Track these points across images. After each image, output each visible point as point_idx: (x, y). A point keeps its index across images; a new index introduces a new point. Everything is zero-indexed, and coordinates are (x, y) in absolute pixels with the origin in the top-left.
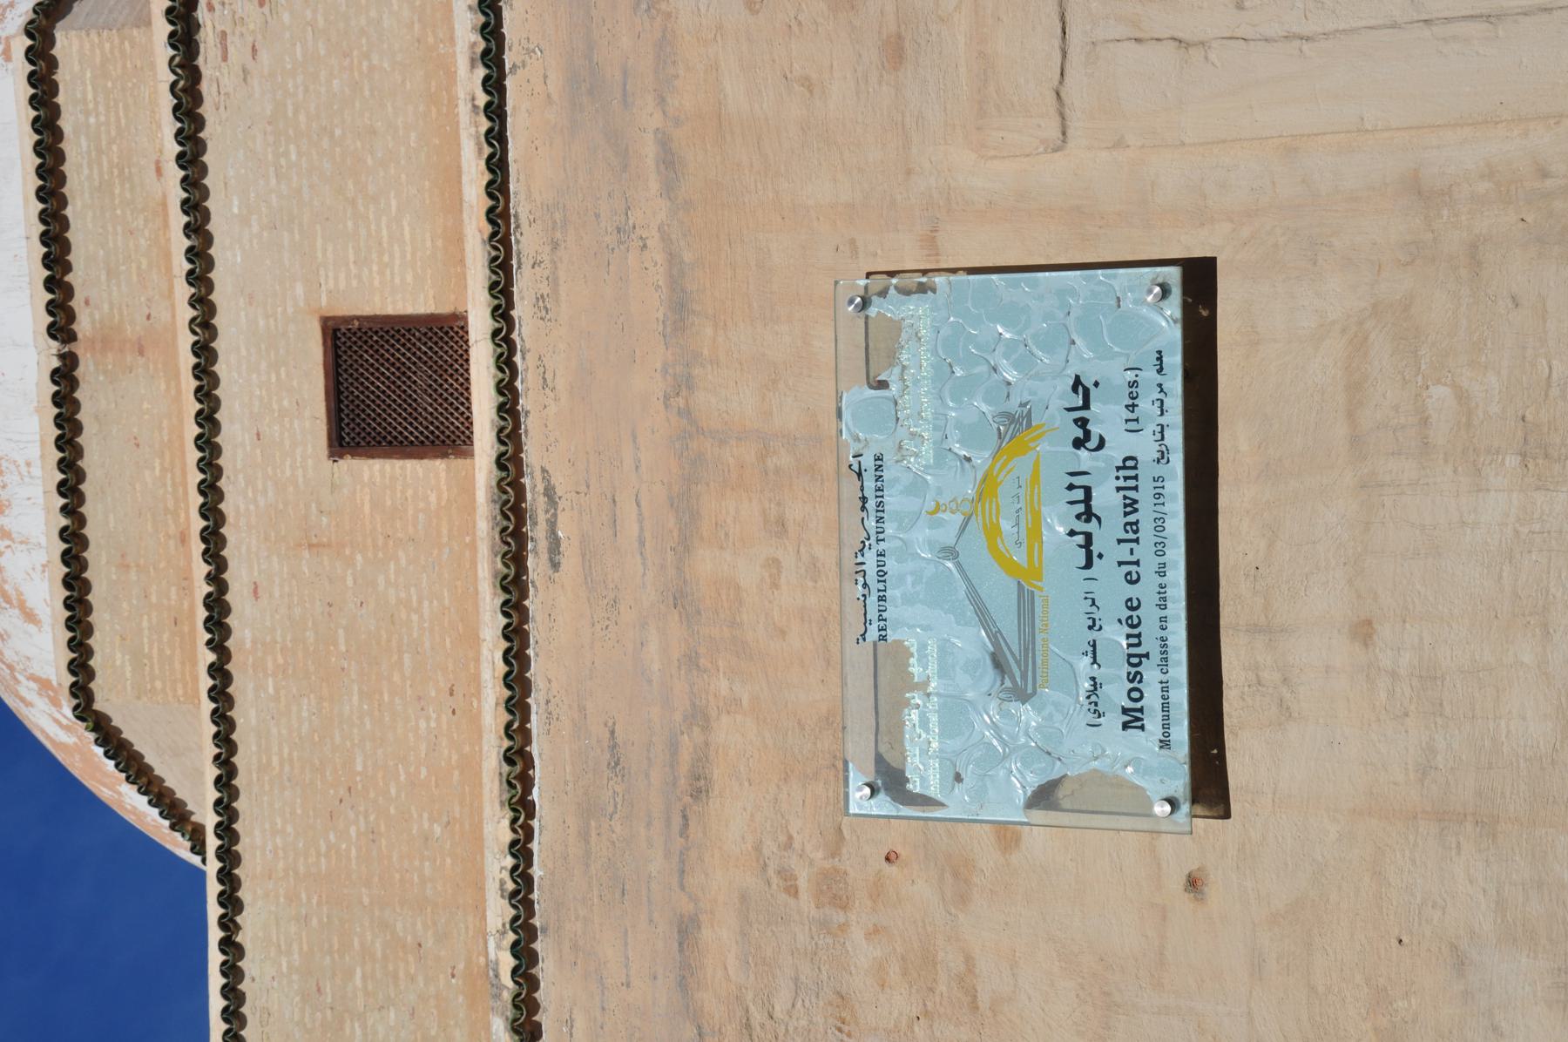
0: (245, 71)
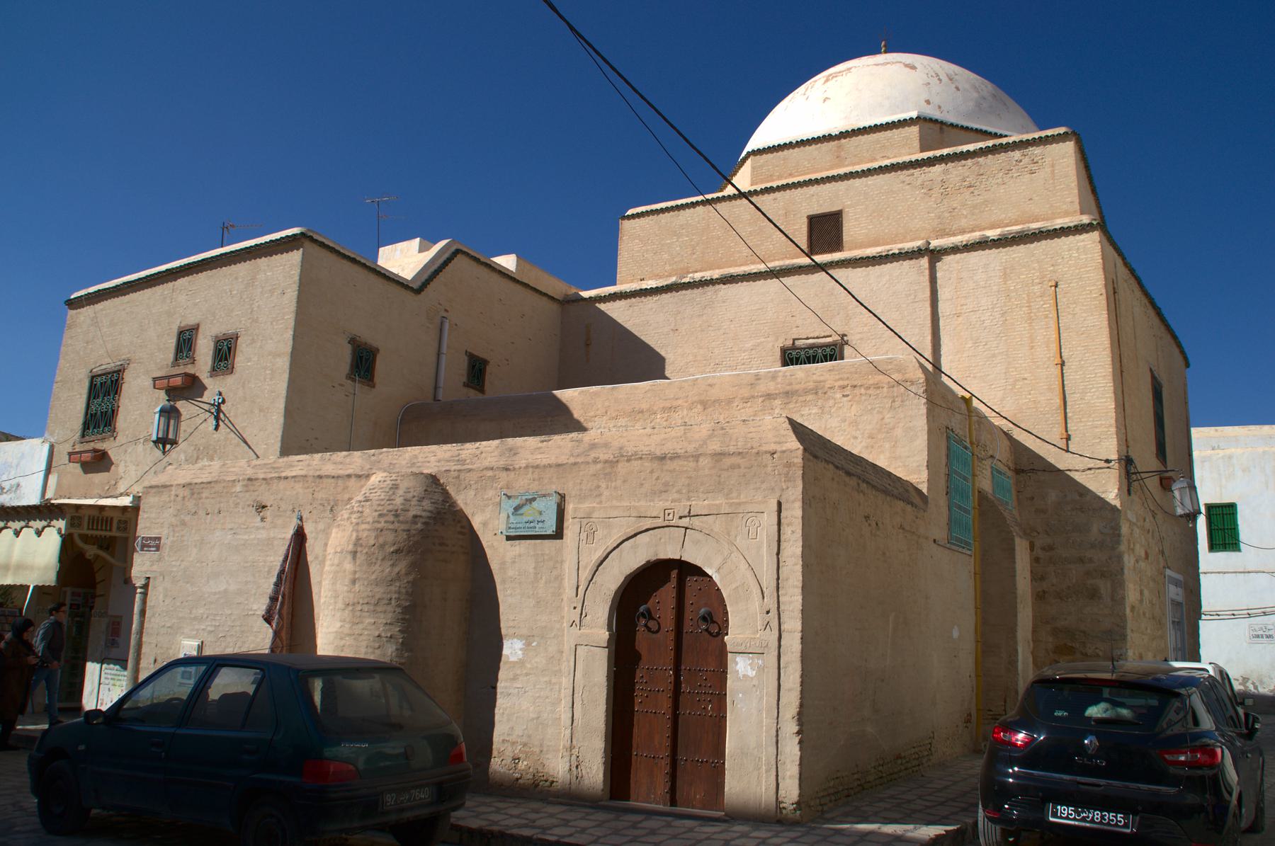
0: (904, 182)
